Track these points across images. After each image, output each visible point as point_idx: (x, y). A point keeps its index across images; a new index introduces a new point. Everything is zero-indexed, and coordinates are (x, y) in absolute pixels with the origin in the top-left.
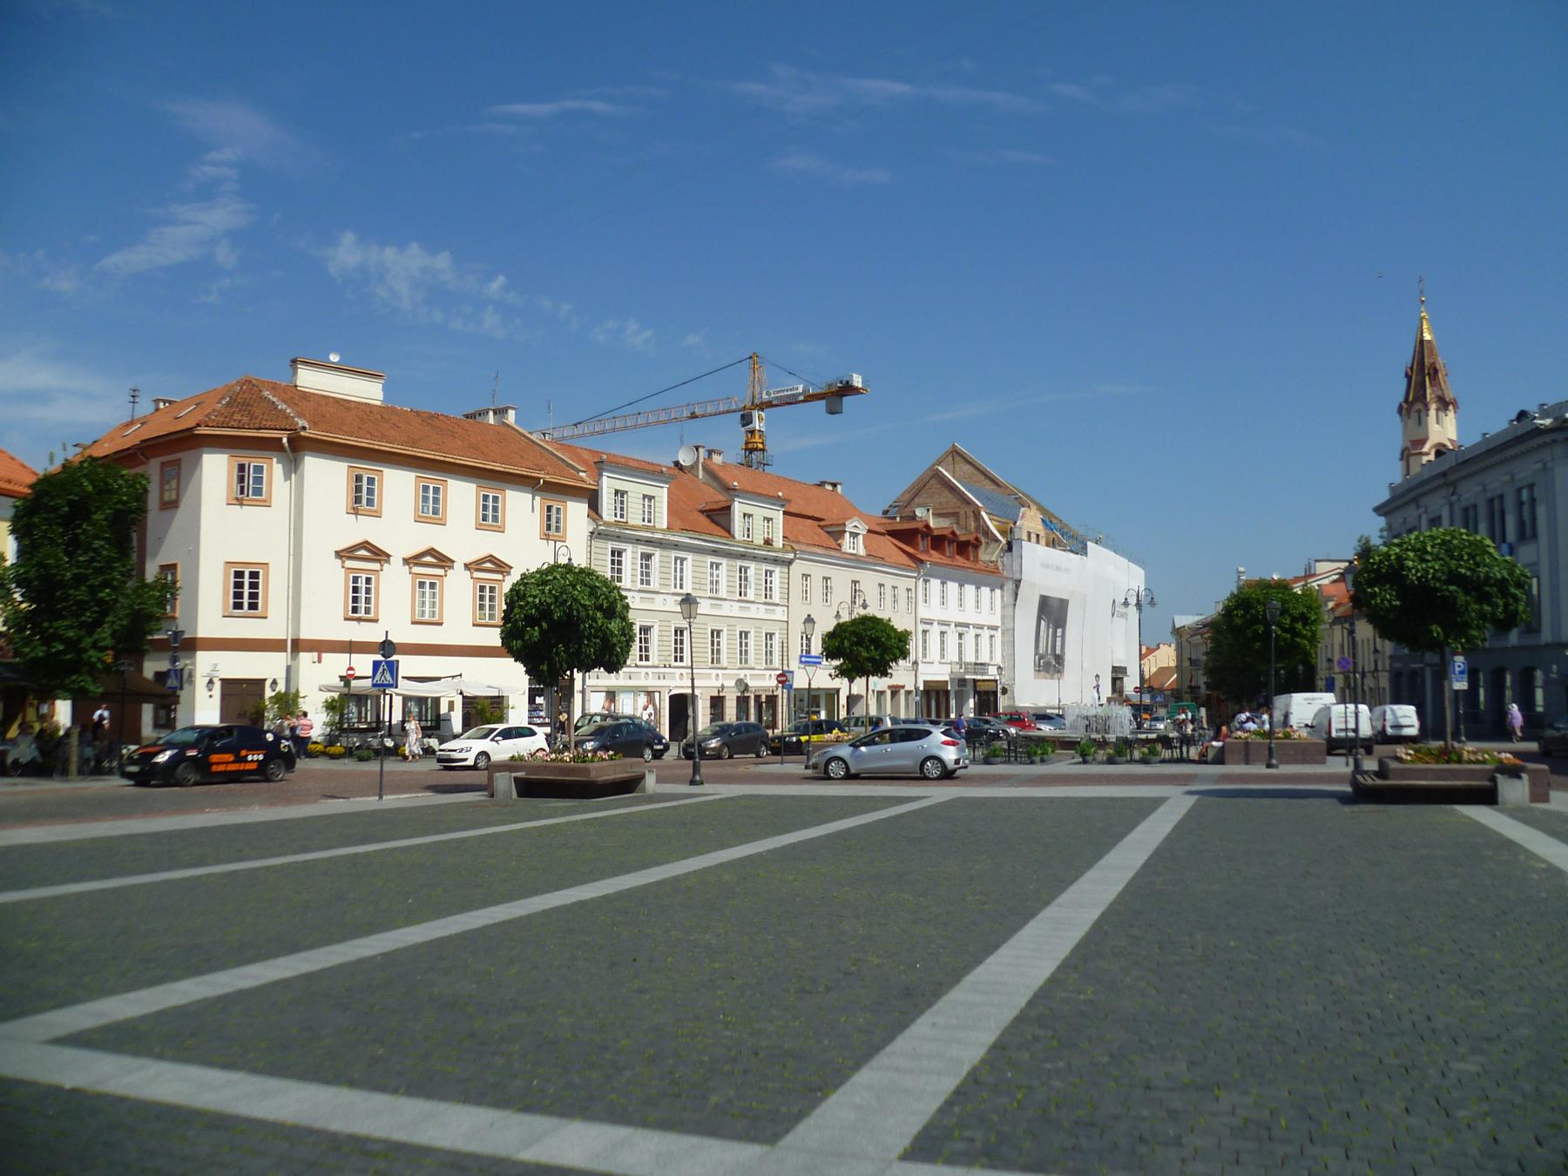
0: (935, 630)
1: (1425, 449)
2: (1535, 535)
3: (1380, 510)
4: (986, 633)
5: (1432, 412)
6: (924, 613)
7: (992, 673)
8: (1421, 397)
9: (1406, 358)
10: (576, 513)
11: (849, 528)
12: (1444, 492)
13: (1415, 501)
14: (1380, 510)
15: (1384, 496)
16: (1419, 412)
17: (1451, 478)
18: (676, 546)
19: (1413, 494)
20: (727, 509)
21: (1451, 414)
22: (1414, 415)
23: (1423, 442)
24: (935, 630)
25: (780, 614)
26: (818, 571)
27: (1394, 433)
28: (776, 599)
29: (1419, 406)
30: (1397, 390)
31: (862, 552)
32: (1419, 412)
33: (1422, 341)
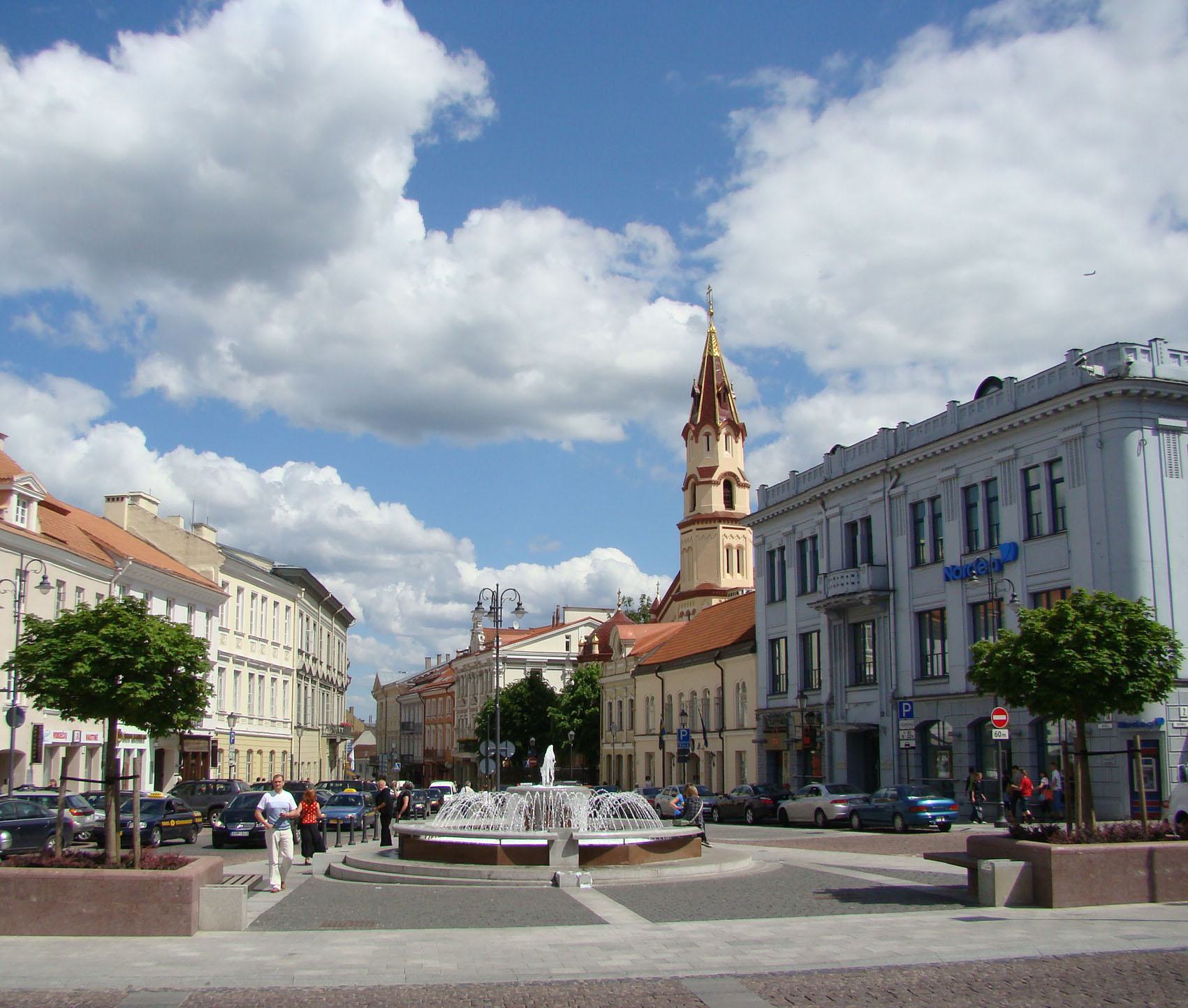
1: (715, 477)
2: (1058, 527)
5: (722, 437)
8: (709, 417)
12: (879, 486)
13: (822, 500)
16: (708, 435)
17: (895, 463)
22: (702, 439)
23: (712, 470)
29: (707, 429)
31: (34, 526)
32: (708, 435)
33: (710, 358)
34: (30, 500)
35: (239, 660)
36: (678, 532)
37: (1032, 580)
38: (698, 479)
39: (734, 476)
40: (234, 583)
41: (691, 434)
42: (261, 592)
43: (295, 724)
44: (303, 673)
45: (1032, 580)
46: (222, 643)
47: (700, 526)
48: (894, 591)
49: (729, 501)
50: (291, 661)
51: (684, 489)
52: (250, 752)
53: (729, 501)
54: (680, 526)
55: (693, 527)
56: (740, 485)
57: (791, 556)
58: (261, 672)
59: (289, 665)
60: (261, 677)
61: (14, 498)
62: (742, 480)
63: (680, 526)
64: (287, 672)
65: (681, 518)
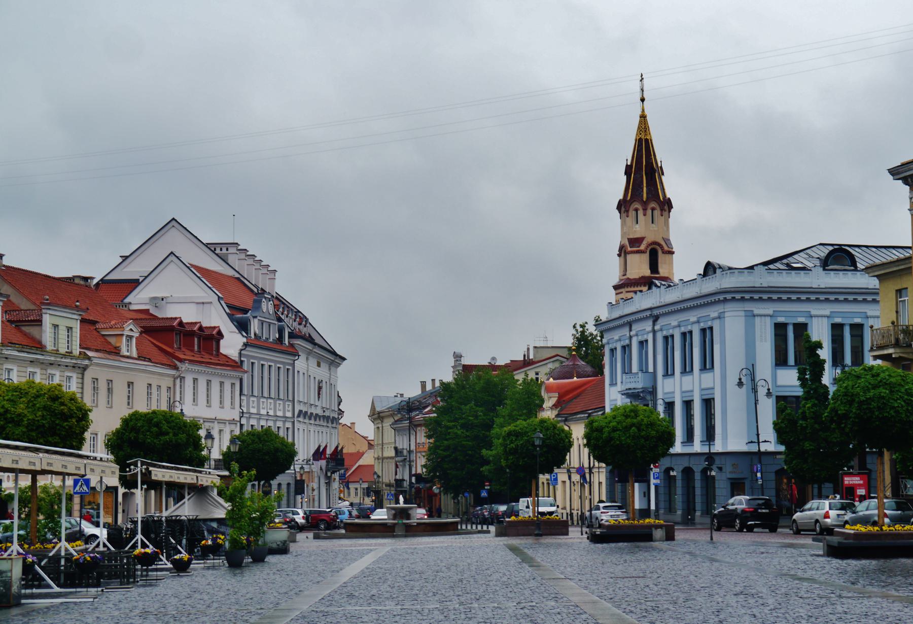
1: (642, 247)
9: (627, 153)
16: (636, 210)
17: (656, 312)
19: (626, 320)
22: (632, 213)
26: (103, 376)
27: (612, 228)
32: (636, 210)
36: (613, 292)
37: (704, 392)
39: (659, 245)
41: (623, 209)
45: (704, 392)
47: (629, 289)
49: (654, 267)
51: (619, 255)
53: (654, 267)
54: (616, 287)
55: (622, 290)
56: (665, 252)
62: (666, 248)
63: (616, 287)
65: (616, 280)
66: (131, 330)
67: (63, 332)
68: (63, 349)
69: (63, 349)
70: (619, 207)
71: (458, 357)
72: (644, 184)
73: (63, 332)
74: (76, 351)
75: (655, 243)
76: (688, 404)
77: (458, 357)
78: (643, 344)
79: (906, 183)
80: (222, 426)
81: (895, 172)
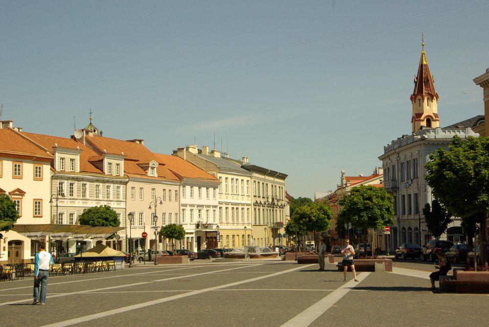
0: (188, 209)
1: (422, 118)
3: (381, 158)
4: (211, 209)
5: (426, 100)
6: (183, 201)
7: (214, 228)
9: (415, 73)
10: (46, 169)
11: (151, 165)
14: (381, 158)
15: (382, 152)
16: (419, 100)
17: (397, 150)
18: (82, 179)
20: (102, 161)
21: (435, 101)
22: (417, 101)
23: (421, 115)
24: (188, 209)
25: (123, 205)
26: (138, 185)
27: (409, 109)
28: (121, 199)
30: (411, 88)
31: (156, 175)
32: (419, 100)
34: (154, 168)
35: (227, 203)
38: (417, 116)
39: (431, 116)
40: (224, 176)
42: (235, 177)
43: (253, 224)
44: (256, 204)
46: (220, 198)
48: (399, 188)
50: (250, 201)
51: (412, 122)
52: (233, 236)
57: (412, 164)
58: (237, 206)
59: (249, 202)
60: (237, 208)
61: (150, 168)
62: (434, 118)
64: (248, 205)
66: (153, 164)
67: (114, 167)
68: (114, 174)
69: (114, 174)
70: (411, 99)
71: (343, 174)
72: (423, 86)
73: (114, 167)
74: (122, 174)
75: (429, 116)
76: (410, 195)
77: (343, 174)
78: (394, 167)
79: (481, 86)
80: (227, 206)
81: (475, 80)
